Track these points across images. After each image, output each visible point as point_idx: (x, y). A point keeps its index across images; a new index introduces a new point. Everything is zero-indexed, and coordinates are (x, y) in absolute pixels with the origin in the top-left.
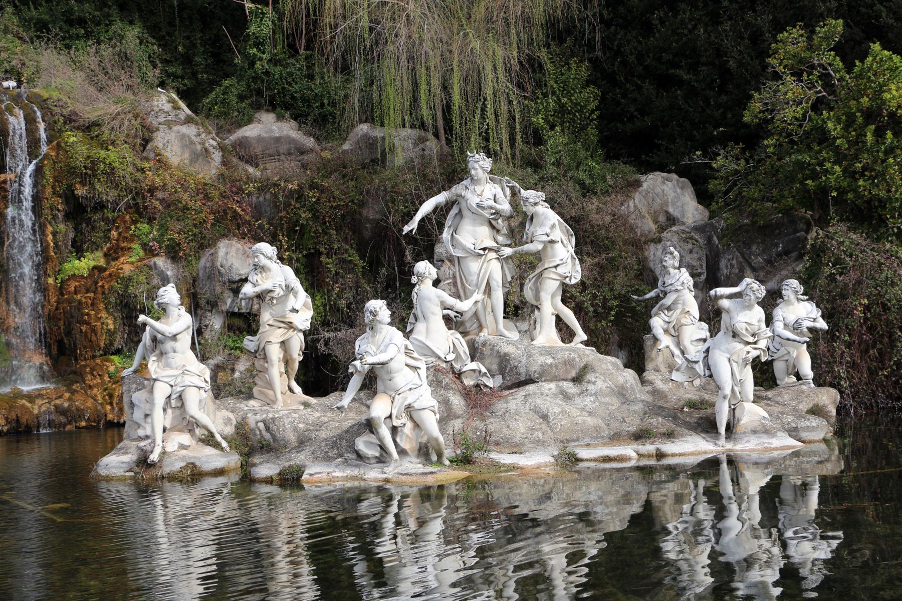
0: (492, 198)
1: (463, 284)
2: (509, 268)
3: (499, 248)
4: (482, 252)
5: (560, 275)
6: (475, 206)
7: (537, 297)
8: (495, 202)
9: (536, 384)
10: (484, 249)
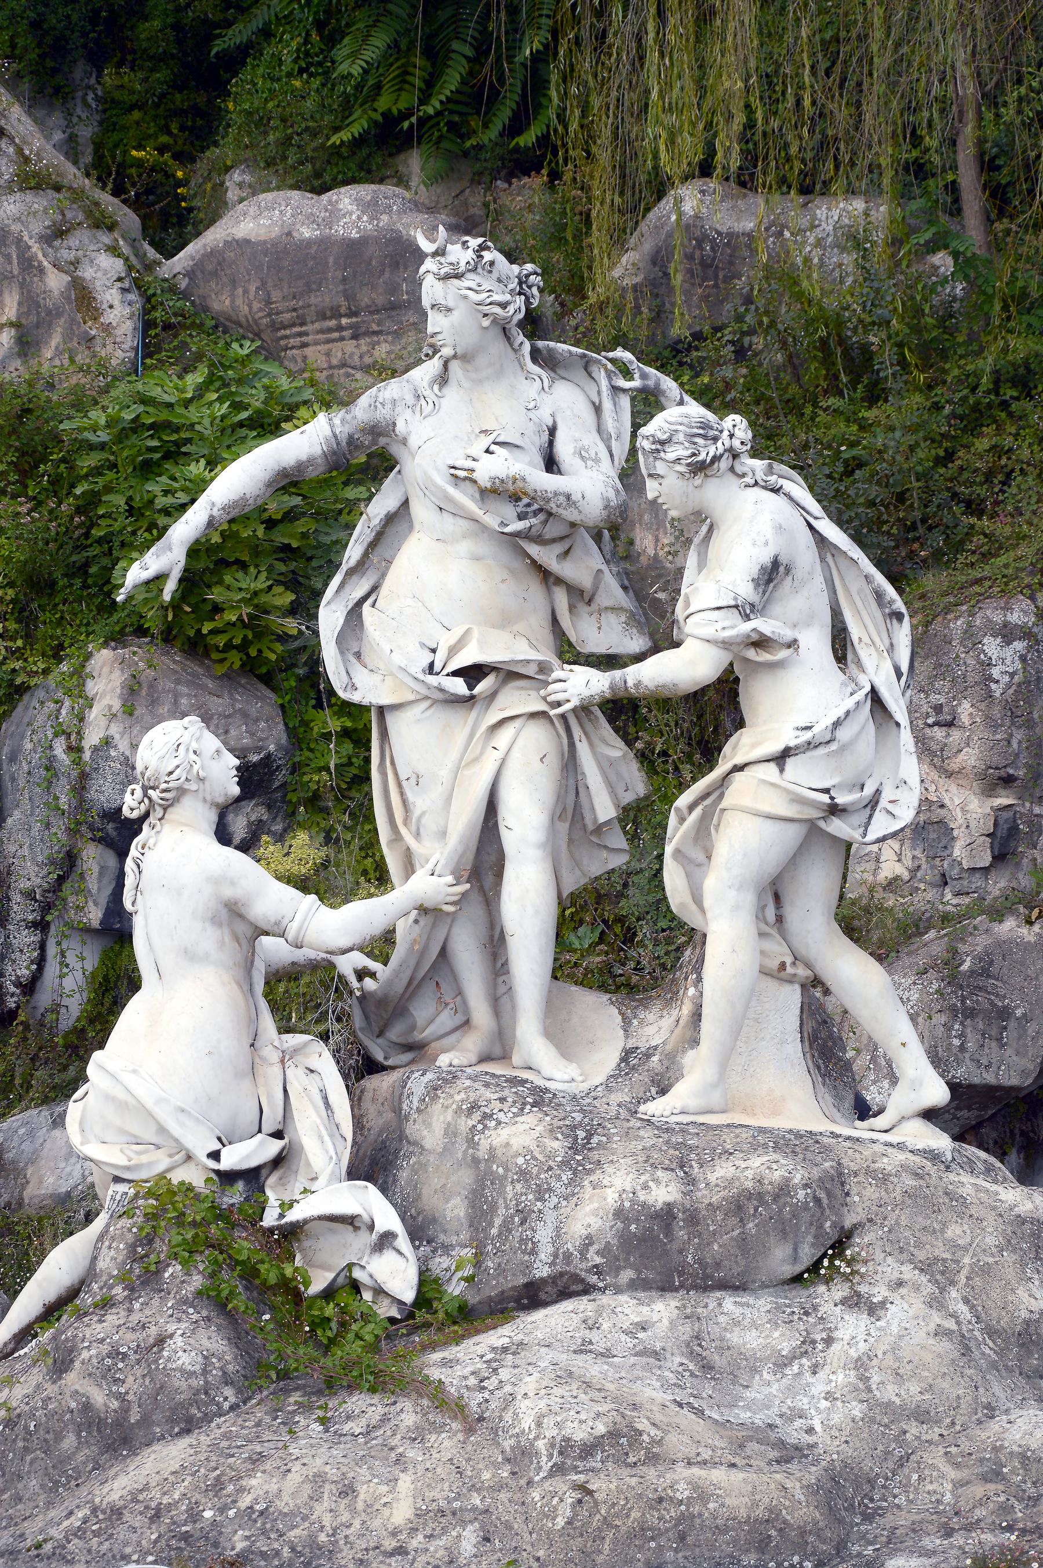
0: (534, 443)
1: (397, 836)
2: (606, 766)
3: (544, 668)
4: (459, 686)
5: (798, 800)
6: (441, 480)
7: (698, 899)
8: (551, 464)
9: (582, 1305)
10: (473, 673)
